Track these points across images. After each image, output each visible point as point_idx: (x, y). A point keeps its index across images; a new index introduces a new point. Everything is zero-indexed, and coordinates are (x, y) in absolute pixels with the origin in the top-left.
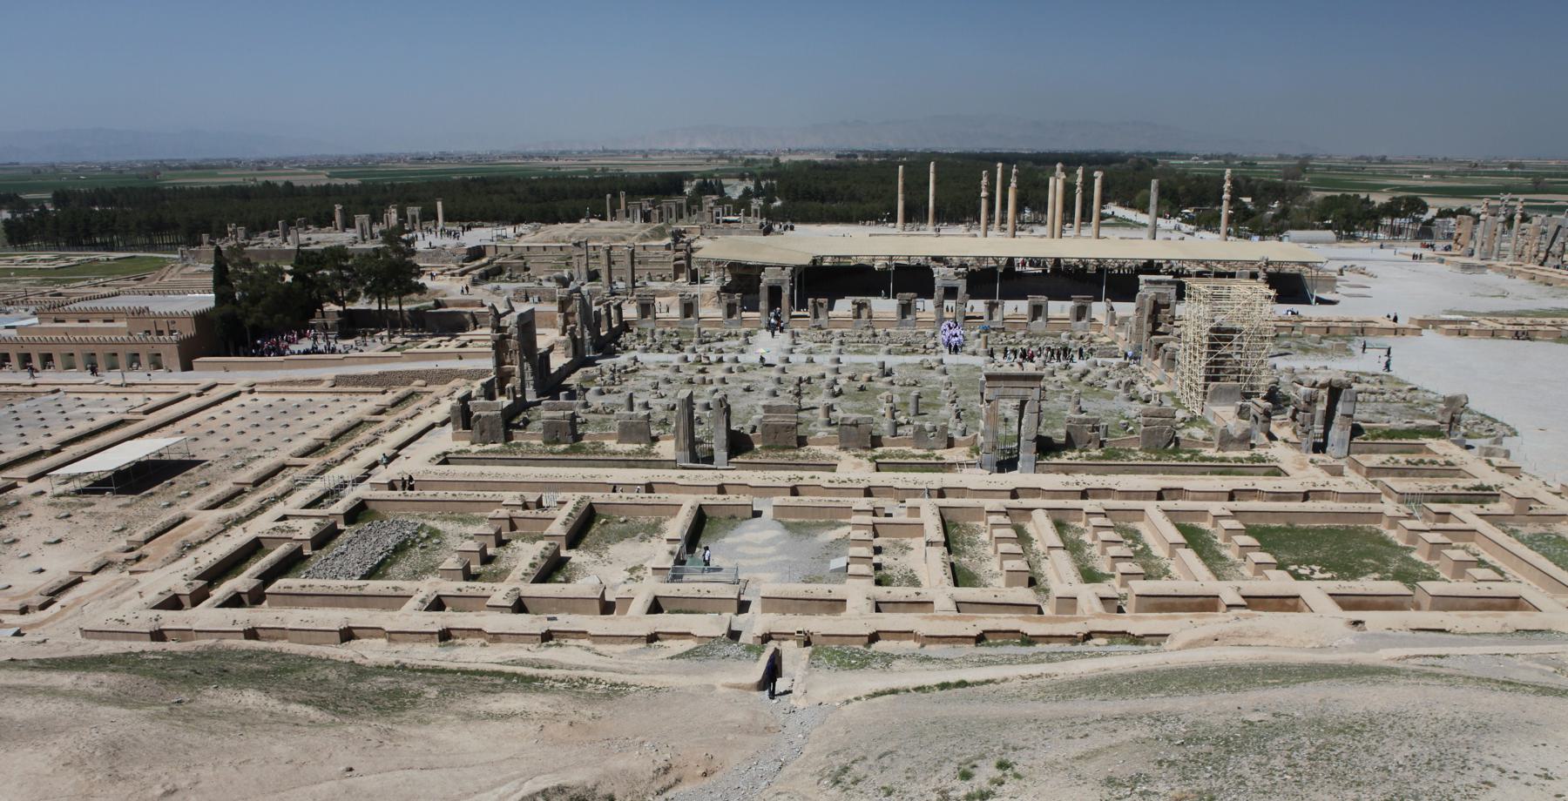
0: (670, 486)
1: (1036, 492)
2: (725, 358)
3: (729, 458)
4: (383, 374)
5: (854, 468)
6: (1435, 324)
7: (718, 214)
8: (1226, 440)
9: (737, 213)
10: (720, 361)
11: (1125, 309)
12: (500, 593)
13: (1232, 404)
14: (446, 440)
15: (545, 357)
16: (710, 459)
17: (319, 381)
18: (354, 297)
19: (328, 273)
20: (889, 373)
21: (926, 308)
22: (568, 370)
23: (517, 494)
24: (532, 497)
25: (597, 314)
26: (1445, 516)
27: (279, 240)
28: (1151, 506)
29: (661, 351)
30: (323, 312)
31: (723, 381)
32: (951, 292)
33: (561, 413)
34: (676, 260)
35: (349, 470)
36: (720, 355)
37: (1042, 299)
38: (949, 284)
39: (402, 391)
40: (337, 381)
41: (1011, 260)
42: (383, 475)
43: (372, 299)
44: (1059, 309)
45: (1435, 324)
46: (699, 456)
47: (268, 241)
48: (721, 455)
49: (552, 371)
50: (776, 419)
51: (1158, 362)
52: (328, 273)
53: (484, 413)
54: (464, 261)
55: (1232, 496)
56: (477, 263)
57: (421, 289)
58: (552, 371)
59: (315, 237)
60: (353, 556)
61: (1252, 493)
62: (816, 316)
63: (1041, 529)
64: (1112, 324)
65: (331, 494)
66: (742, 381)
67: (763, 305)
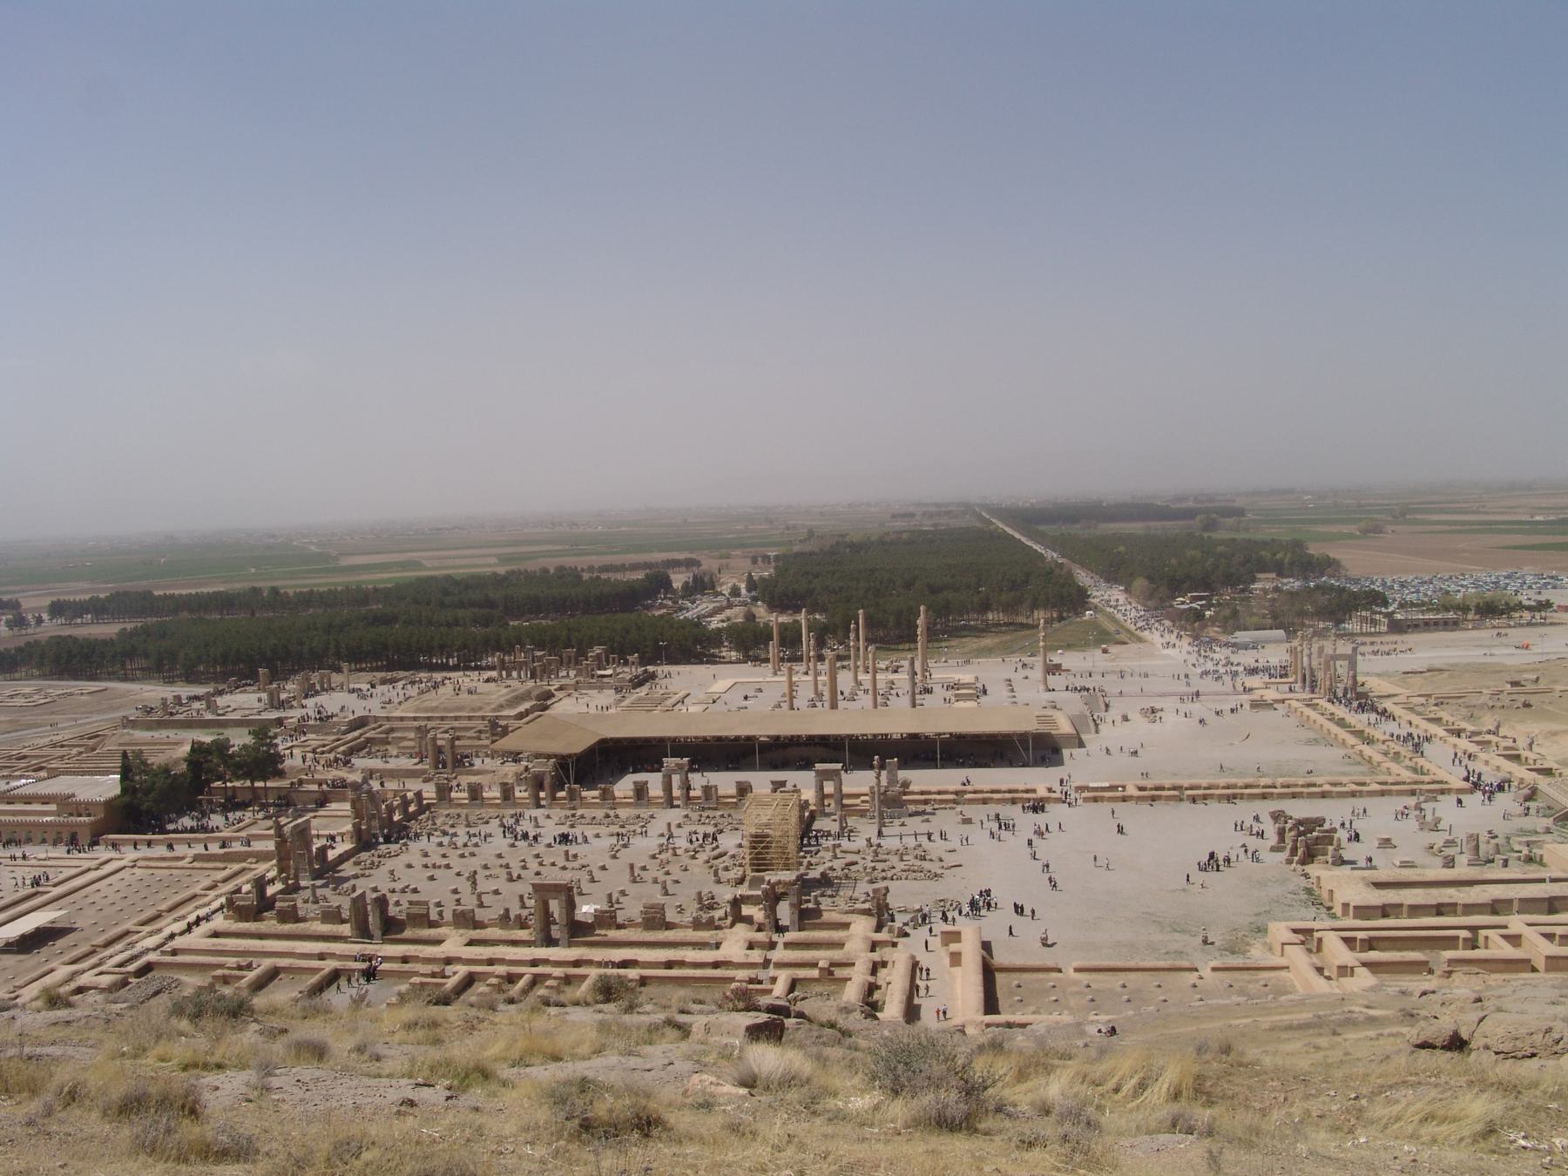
3: (383, 935)
5: (454, 943)
7: (593, 670)
14: (219, 922)
16: (371, 937)
23: (235, 959)
24: (243, 961)
30: (210, 787)
33: (286, 904)
35: (150, 942)
39: (236, 867)
46: (364, 932)
48: (377, 933)
50: (415, 910)
53: (242, 903)
61: (681, 964)
62: (572, 796)
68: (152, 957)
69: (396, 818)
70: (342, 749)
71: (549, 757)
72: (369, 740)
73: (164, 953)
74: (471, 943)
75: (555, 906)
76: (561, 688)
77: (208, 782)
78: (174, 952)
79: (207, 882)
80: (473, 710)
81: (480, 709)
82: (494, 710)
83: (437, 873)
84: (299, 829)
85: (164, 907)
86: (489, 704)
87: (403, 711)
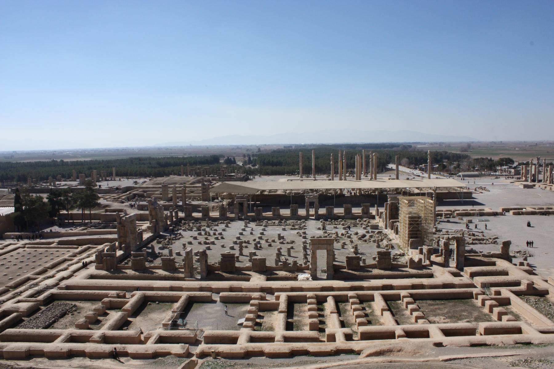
0: (180, 289)
1: (331, 289)
2: (217, 233)
4: (77, 240)
6: (508, 210)
8: (413, 264)
9: (234, 173)
10: (215, 234)
11: (382, 210)
12: (97, 333)
13: (417, 249)
15: (141, 234)
17: (53, 243)
18: (72, 208)
19: (62, 198)
20: (283, 238)
21: (302, 212)
22: (150, 240)
24: (122, 293)
25: (166, 215)
26: (498, 293)
27: (48, 184)
28: (377, 294)
29: (192, 230)
31: (213, 243)
32: (311, 205)
34: (203, 192)
35: (50, 282)
36: (215, 232)
37: (349, 205)
38: (311, 200)
40: (60, 243)
41: (341, 190)
42: (63, 284)
43: (80, 208)
44: (357, 211)
45: (508, 210)
47: (45, 184)
49: (144, 239)
51: (393, 231)
52: (62, 198)
54: (120, 193)
55: (414, 287)
56: (124, 194)
57: (99, 206)
58: (144, 239)
59: (63, 183)
60: (42, 319)
63: (330, 305)
64: (378, 215)
65: (39, 293)
66: (222, 243)
67: (236, 210)
68: (54, 291)
69: (169, 223)
70: (124, 197)
71: (244, 195)
72: (135, 195)
73: (61, 288)
74: (268, 279)
75: (322, 255)
76: (213, 180)
77: (58, 210)
78: (68, 288)
79: (70, 254)
80: (181, 184)
81: (185, 183)
82: (191, 184)
83: (212, 246)
84: (131, 219)
85: (48, 265)
86: (188, 182)
87: (146, 185)
